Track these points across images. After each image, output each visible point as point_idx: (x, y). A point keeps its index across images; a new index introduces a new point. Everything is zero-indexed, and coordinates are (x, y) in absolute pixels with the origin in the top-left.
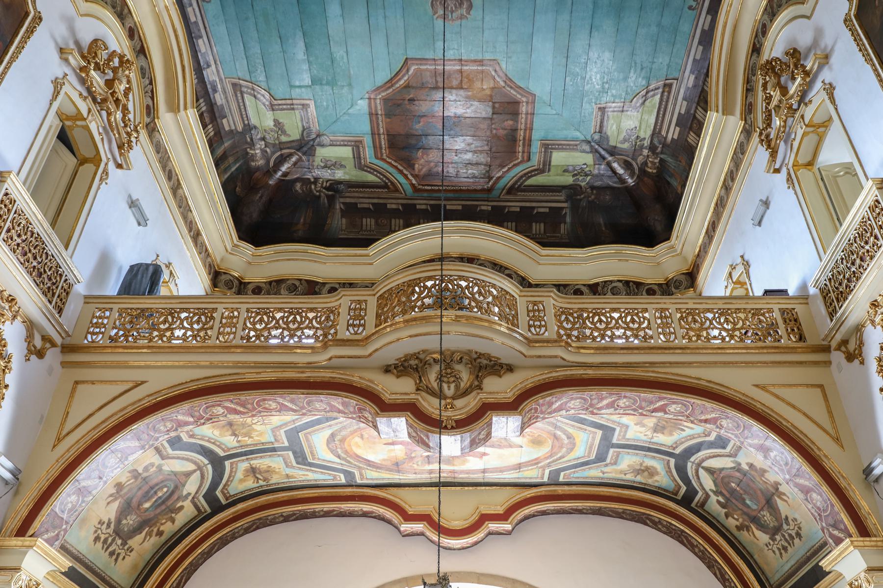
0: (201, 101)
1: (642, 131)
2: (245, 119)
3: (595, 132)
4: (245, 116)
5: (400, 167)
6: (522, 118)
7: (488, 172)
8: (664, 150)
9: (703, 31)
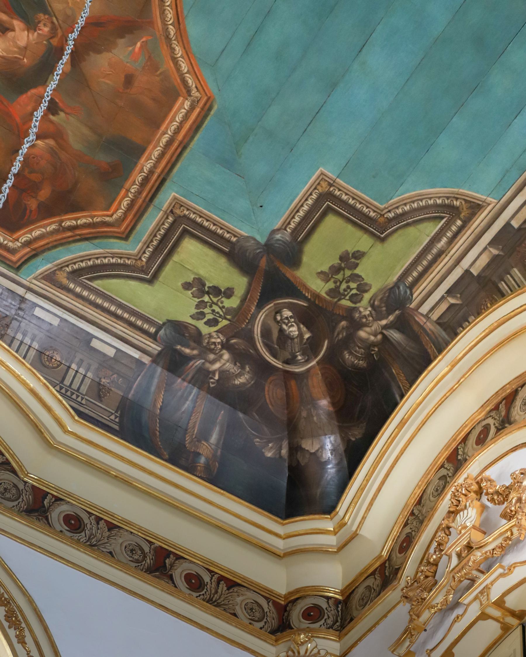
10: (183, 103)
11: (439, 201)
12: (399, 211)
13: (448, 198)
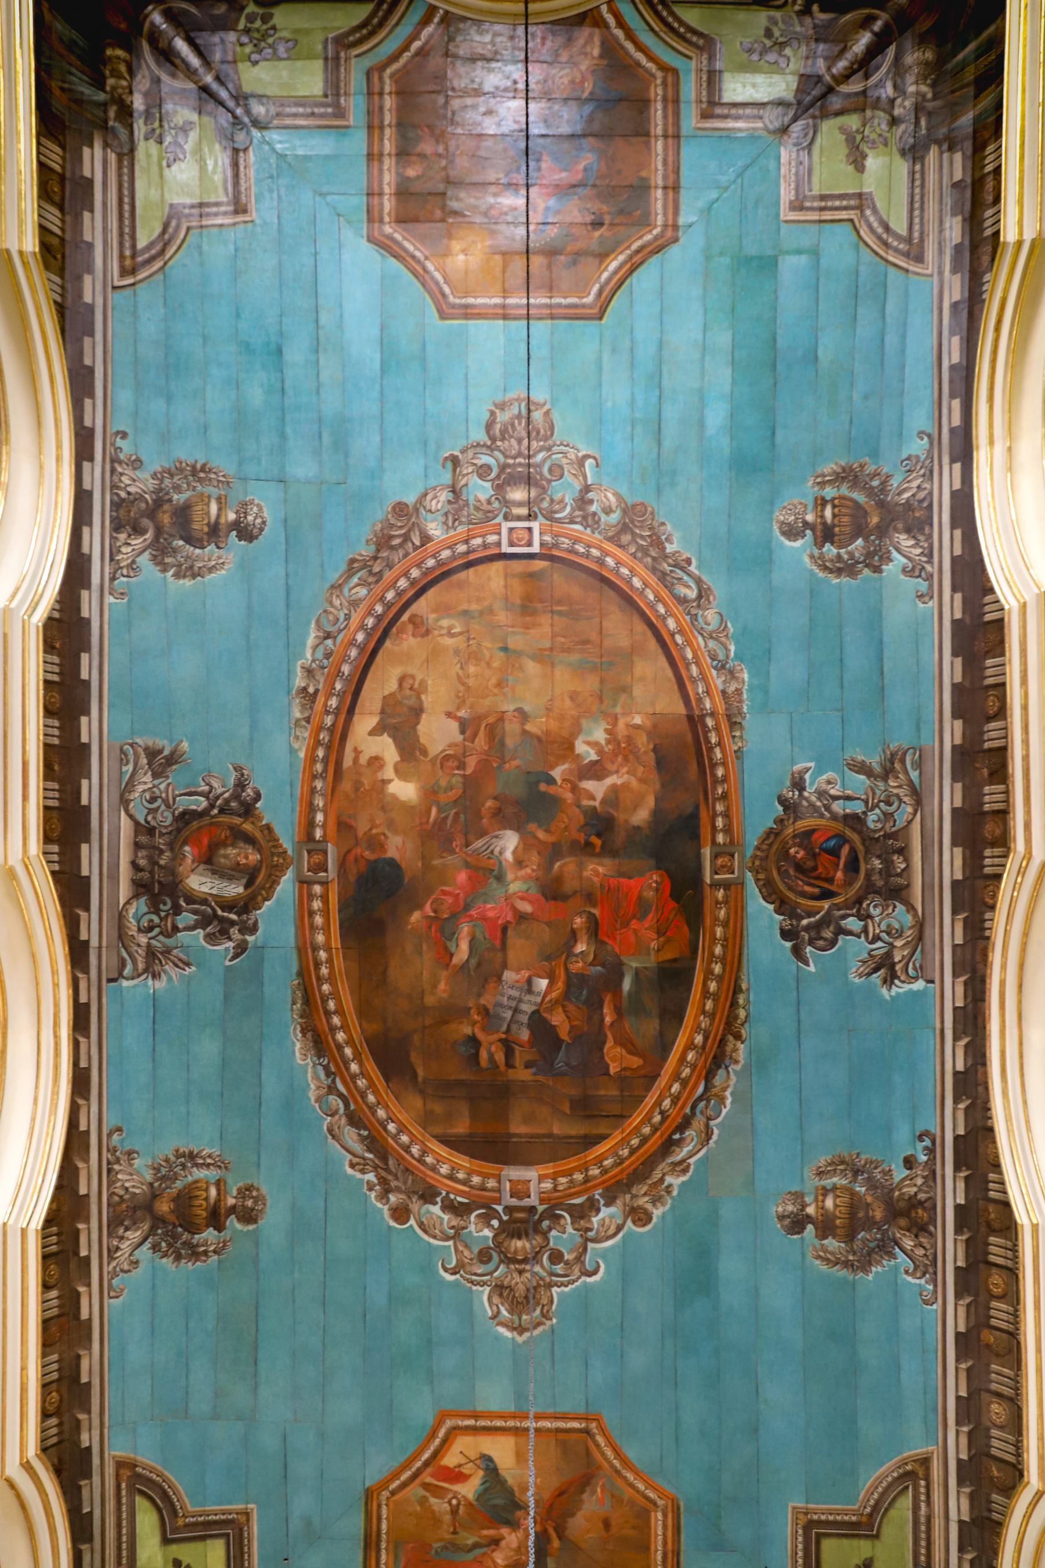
0: (988, 232)
1: (155, 159)
2: (918, 176)
3: (245, 150)
4: (918, 183)
5: (629, 46)
6: (389, 184)
7: (451, 39)
8: (102, 114)
9: (92, 395)
10: (656, 1517)
11: (895, 1475)
12: (872, 1502)
13: (899, 1467)
